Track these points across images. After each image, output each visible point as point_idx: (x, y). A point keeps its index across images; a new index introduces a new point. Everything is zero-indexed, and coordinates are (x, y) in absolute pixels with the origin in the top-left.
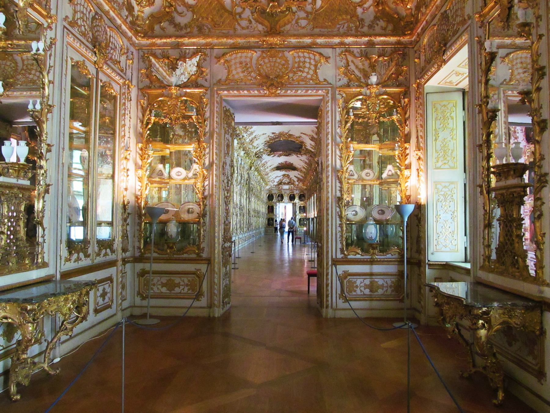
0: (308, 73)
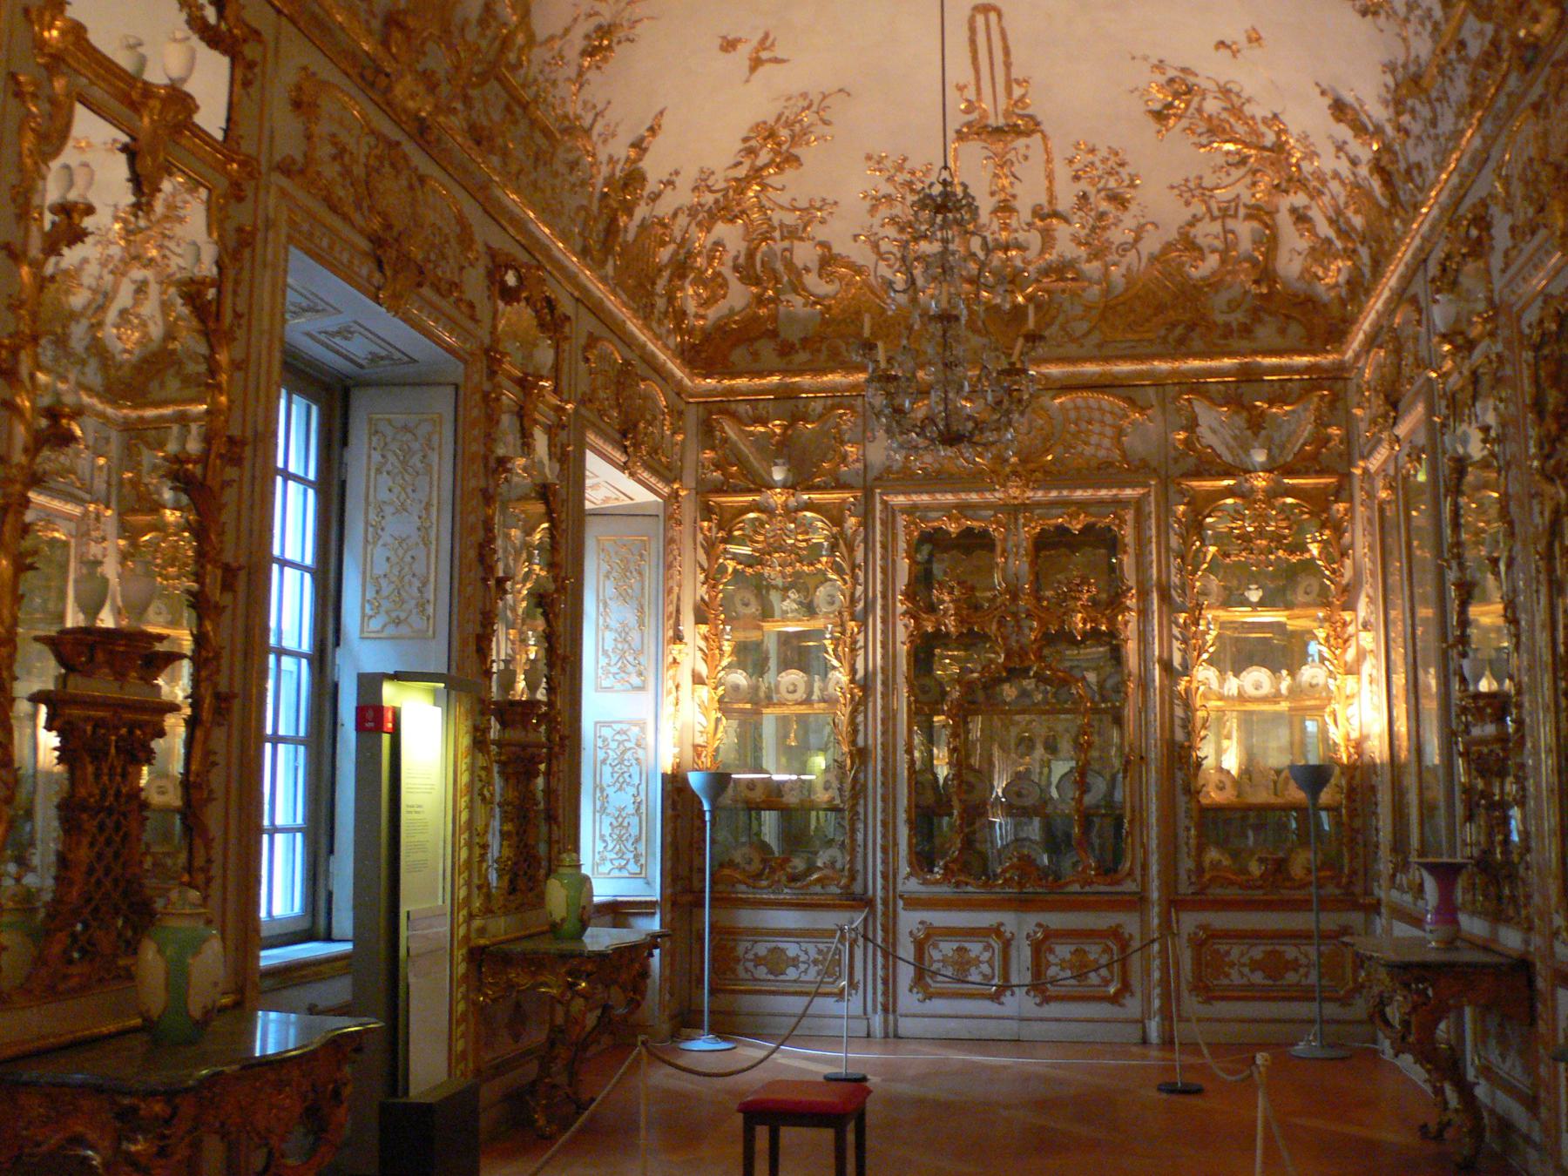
0: (1099, 446)
